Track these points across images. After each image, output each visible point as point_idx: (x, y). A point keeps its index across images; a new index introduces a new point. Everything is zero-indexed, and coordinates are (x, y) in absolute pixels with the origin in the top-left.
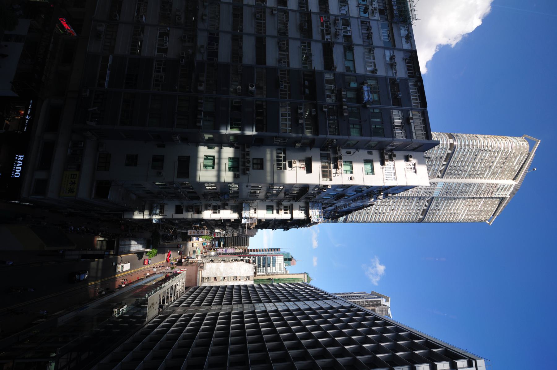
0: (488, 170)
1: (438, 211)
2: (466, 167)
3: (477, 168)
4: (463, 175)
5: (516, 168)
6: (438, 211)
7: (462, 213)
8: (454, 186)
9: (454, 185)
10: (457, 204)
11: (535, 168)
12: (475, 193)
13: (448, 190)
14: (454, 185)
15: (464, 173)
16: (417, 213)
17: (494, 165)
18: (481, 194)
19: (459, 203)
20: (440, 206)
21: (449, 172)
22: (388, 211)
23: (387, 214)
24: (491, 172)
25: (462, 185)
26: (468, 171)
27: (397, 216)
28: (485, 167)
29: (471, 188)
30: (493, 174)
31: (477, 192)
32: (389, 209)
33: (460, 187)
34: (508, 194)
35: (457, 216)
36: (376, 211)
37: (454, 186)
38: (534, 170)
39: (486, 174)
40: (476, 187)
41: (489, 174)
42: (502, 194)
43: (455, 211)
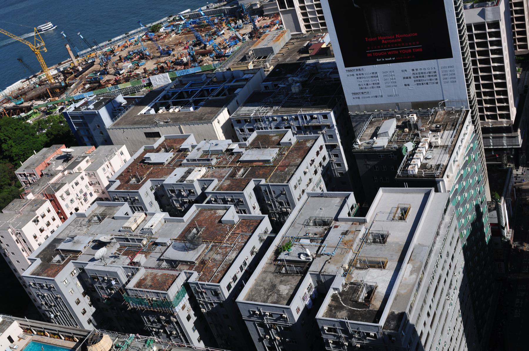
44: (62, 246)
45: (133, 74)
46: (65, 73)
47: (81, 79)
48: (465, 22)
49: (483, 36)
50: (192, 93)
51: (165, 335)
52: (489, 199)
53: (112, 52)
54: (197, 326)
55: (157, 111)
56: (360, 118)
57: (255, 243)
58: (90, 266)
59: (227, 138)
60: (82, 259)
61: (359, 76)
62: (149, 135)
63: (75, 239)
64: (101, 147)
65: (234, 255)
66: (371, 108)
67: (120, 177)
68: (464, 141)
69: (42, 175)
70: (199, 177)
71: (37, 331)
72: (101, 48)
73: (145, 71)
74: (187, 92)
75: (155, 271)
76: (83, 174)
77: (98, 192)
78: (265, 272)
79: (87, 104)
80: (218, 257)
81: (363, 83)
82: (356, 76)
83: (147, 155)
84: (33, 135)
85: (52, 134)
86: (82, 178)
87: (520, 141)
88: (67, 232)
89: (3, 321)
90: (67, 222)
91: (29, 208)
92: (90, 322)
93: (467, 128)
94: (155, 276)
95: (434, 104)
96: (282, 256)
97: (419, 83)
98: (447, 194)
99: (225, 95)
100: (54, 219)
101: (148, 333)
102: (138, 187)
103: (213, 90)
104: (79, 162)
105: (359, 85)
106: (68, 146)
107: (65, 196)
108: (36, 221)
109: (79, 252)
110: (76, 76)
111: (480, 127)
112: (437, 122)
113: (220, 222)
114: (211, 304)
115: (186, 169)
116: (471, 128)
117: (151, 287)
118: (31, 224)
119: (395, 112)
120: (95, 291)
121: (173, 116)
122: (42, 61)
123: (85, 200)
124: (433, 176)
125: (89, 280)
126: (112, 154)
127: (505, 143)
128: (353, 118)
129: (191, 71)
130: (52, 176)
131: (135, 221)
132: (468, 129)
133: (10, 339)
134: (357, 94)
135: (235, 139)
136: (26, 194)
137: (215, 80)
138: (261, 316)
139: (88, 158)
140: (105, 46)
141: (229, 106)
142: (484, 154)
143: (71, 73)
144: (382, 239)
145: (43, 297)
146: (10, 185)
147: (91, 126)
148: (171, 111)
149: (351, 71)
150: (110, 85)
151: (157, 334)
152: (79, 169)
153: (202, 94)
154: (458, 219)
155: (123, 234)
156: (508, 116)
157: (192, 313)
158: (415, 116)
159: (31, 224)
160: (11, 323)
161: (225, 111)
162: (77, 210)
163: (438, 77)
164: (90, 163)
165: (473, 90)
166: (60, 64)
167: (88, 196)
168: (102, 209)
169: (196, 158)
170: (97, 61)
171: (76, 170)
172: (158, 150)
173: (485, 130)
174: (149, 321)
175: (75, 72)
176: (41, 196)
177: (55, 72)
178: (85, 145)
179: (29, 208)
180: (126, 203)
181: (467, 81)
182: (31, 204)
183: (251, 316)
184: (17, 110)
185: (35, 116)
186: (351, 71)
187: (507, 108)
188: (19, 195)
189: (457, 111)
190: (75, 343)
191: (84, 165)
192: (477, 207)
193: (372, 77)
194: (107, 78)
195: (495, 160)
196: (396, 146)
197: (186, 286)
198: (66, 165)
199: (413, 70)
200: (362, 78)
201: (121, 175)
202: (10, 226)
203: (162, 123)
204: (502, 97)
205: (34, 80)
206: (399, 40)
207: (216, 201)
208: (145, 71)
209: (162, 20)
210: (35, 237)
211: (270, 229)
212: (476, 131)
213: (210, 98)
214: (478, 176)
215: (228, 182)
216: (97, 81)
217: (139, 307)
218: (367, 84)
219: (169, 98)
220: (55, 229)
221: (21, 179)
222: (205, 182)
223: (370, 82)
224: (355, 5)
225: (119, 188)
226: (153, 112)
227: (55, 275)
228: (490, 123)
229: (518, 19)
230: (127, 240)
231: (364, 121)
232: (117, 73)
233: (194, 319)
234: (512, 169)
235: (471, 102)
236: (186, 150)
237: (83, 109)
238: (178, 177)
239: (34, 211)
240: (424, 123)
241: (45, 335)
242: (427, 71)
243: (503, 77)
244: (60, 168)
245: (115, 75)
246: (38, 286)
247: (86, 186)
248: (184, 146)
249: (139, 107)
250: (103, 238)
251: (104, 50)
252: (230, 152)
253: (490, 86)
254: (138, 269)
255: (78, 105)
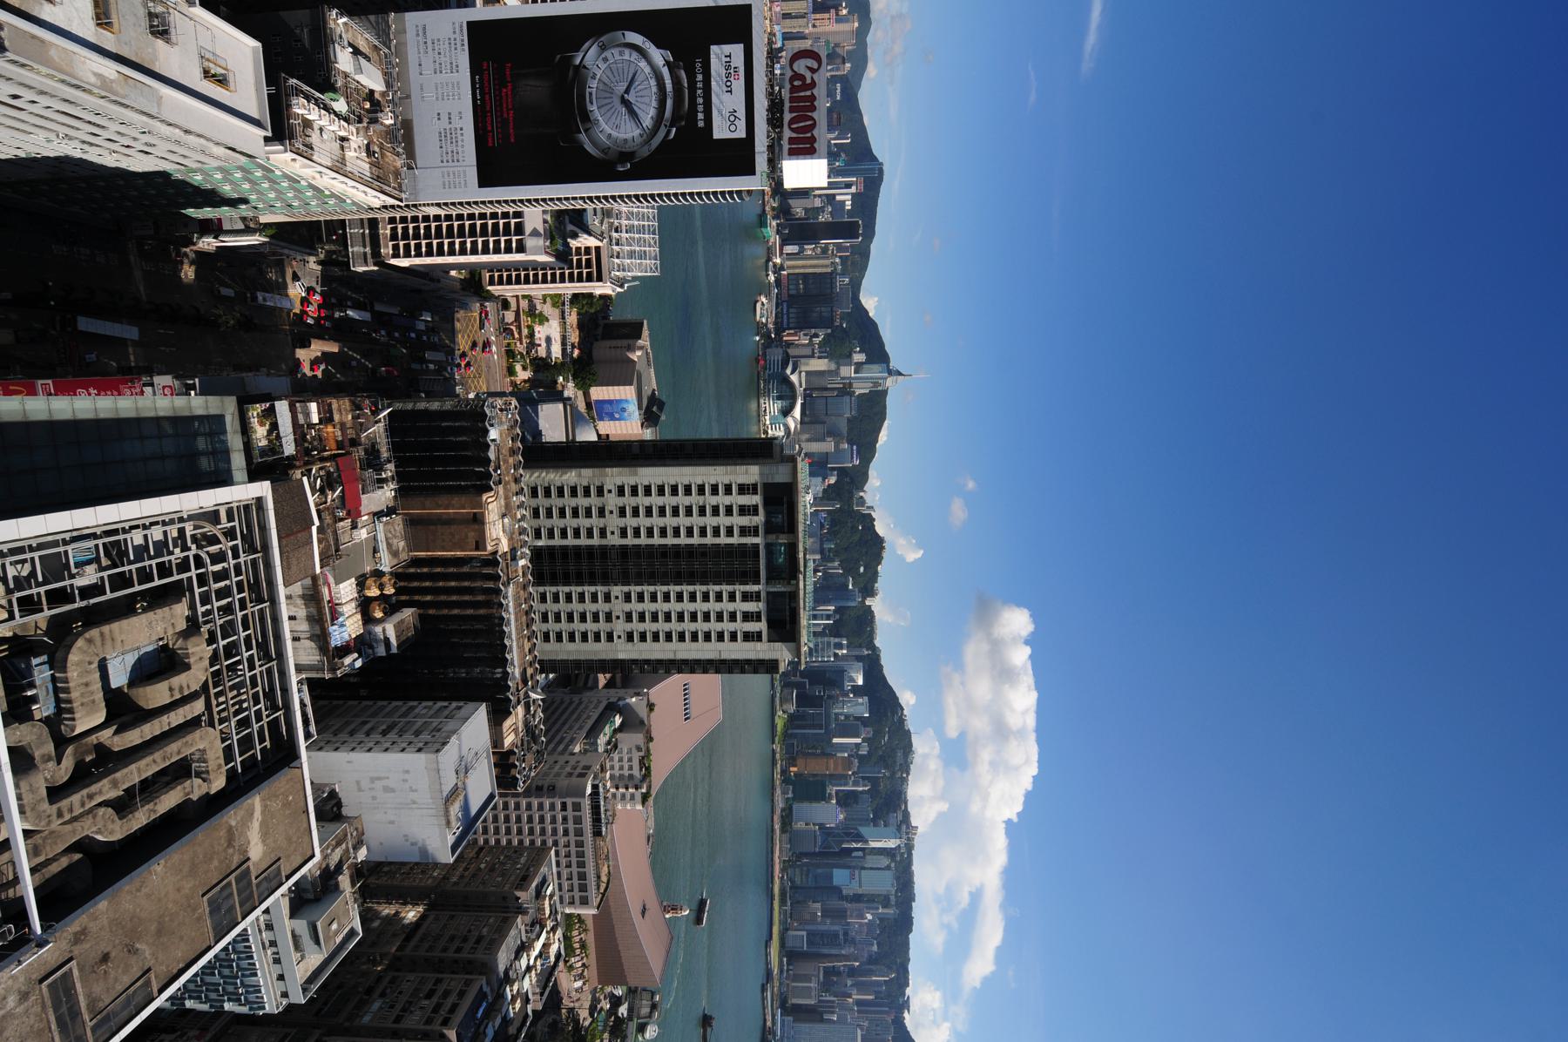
48: (524, 209)
49: (507, 231)
52: (264, 219)
56: (384, 31)
61: (453, 42)
66: (400, 51)
68: (354, 191)
81: (442, 47)
82: (452, 37)
87: (361, 269)
93: (375, 197)
95: (410, 153)
97: (444, 136)
98: (264, 156)
105: (439, 40)
111: (377, 216)
112: (383, 155)
116: (376, 203)
119: (396, 92)
124: (291, 137)
127: (355, 249)
128: (383, 18)
132: (374, 199)
134: (425, 33)
142: (335, 218)
144: (160, 30)
149: (461, 30)
154: (220, 169)
156: (396, 255)
158: (392, 122)
163: (451, 164)
165: (433, 211)
173: (373, 223)
181: (446, 204)
186: (461, 30)
187: (407, 255)
189: (400, 185)
192: (245, 201)
193: (451, 63)
195: (329, 235)
196: (339, 84)
199: (461, 129)
200: (450, 51)
204: (424, 249)
206: (505, 115)
212: (372, 209)
214: (300, 207)
218: (439, 53)
223: (443, 59)
224: (559, 56)
228: (385, 231)
229: (527, 276)
231: (378, 36)
234: (317, 255)
235: (415, 206)
240: (380, 135)
242: (460, 149)
243: (452, 253)
253: (439, 234)
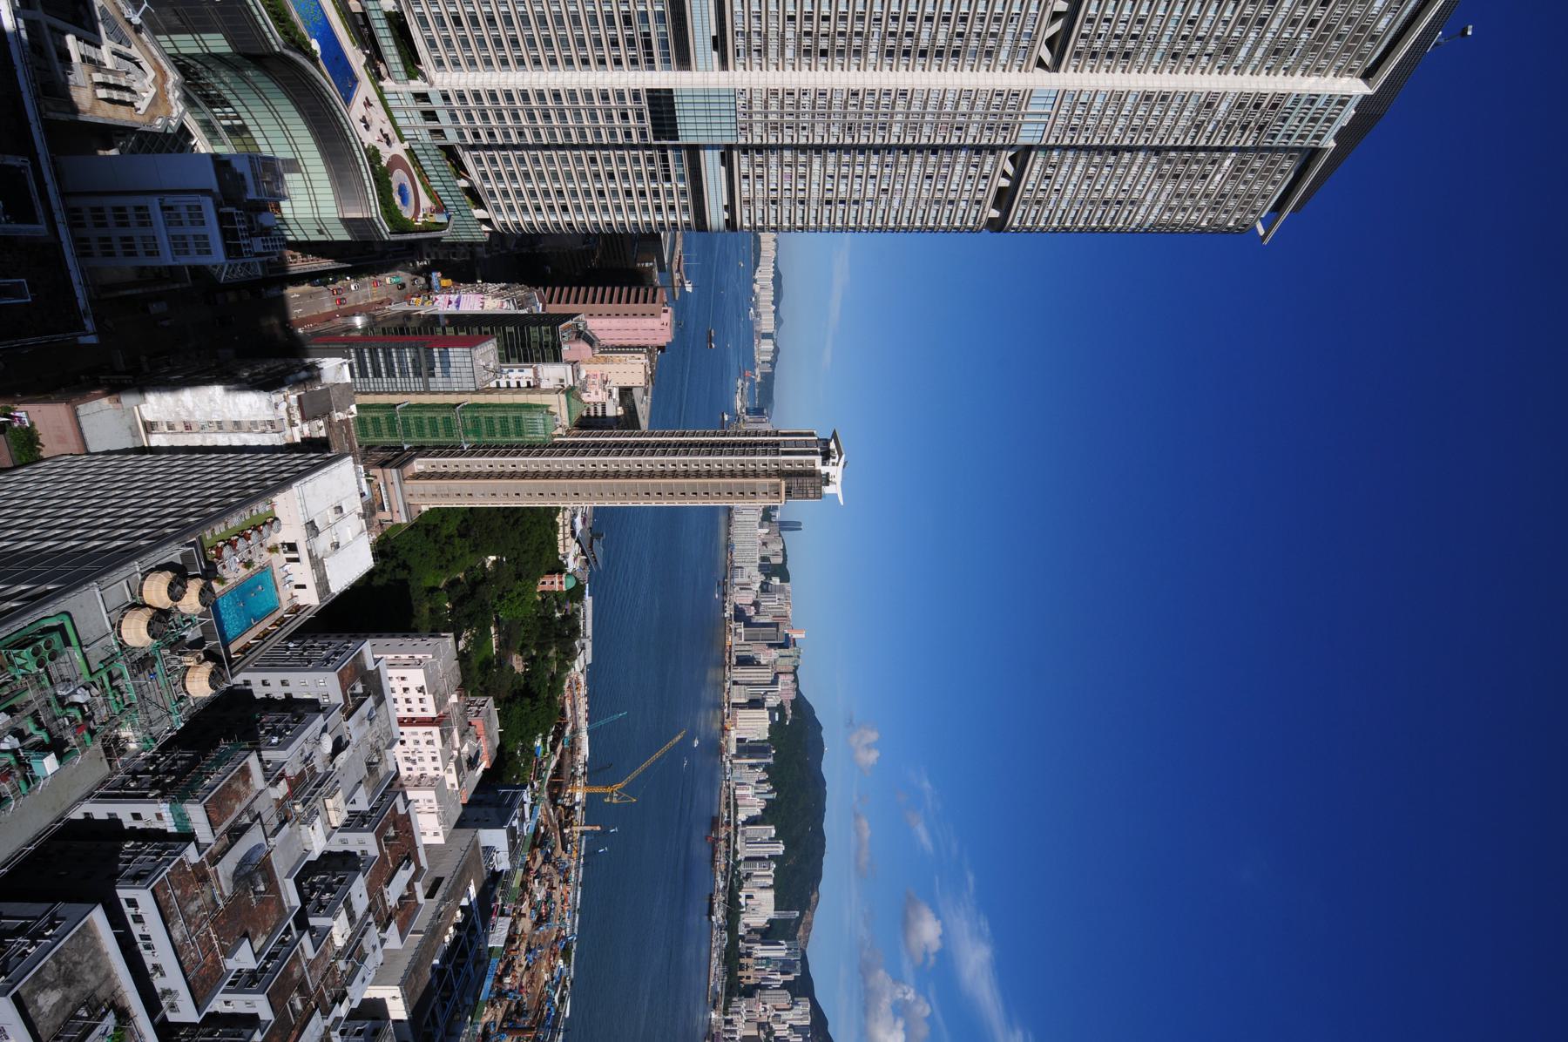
0: (1252, 35)
1: (1054, 196)
2: (1156, 23)
3: (1206, 24)
4: (1143, 55)
5: (1383, 24)
6: (1054, 196)
7: (1147, 203)
8: (1098, 104)
9: (1099, 100)
10: (1128, 167)
11: (1470, 27)
12: (1189, 128)
13: (1075, 121)
14: (1099, 100)
15: (1146, 47)
16: (978, 202)
17: (1281, 14)
18: (1212, 133)
19: (1135, 169)
20: (1060, 179)
21: (1082, 43)
22: (870, 195)
23: (868, 205)
24: (1265, 45)
25: (1130, 99)
26: (1165, 39)
27: (1059, 213)
28: (1243, 21)
29: (1171, 113)
30: (1277, 52)
31: (1198, 127)
32: (870, 187)
33: (1123, 105)
34: (1330, 131)
35: (1130, 212)
36: (828, 195)
37: (1098, 104)
38: (1465, 30)
39: (1243, 53)
40: (1190, 106)
41: (1259, 54)
42: (1301, 137)
43: (1122, 196)
44: (370, 702)
45: (527, 896)
46: (570, 810)
47: (554, 826)
50: (457, 973)
51: (140, 769)
53: (566, 881)
54: (114, 822)
55: (463, 909)
57: (171, 979)
58: (320, 721)
59: (364, 1001)
60: (337, 716)
62: (437, 882)
63: (368, 723)
64: (460, 810)
65: (177, 935)
67: (407, 818)
69: (470, 724)
70: (334, 931)
71: (286, 619)
72: (577, 868)
73: (522, 915)
74: (462, 965)
75: (246, 802)
76: (441, 773)
77: (407, 779)
78: (109, 976)
79: (522, 819)
80: (193, 907)
83: (413, 868)
84: (522, 738)
85: (510, 759)
86: (436, 769)
88: (383, 717)
89: (329, 591)
90: (395, 723)
91: (441, 690)
92: (247, 683)
94: (240, 800)
96: (110, 1021)
99: (428, 1024)
100: (409, 710)
101: (163, 749)
102: (378, 836)
103: (444, 1007)
104: (458, 775)
106: (485, 771)
107: (429, 737)
108: (421, 690)
109: (348, 718)
110: (560, 821)
113: (246, 935)
114: (129, 861)
115: (359, 916)
117: (229, 785)
118: (422, 682)
120: (282, 711)
121: (442, 927)
122: (597, 790)
123: (407, 759)
125: (302, 711)
126: (443, 820)
129: (488, 983)
130: (462, 736)
131: (336, 809)
133: (303, 587)
135: (353, 1015)
136: (459, 696)
137: (457, 1017)
138: (35, 937)
139: (457, 788)
140: (577, 875)
141: (407, 1024)
143: (566, 817)
145: (323, 648)
146: (481, 684)
147: (492, 811)
148: (451, 930)
150: (528, 858)
151: (153, 760)
152: (450, 771)
153: (448, 988)
155: (331, 784)
157: (139, 825)
159: (422, 682)
160: (320, 599)
161: (403, 1015)
162: (403, 742)
164: (449, 787)
166: (584, 809)
167: (409, 765)
168: (382, 772)
169: (365, 939)
170: (565, 857)
171: (452, 766)
172: (410, 886)
174: (181, 759)
175: (566, 821)
176: (447, 710)
177: (577, 799)
178: (474, 793)
179: (441, 690)
180: (368, 809)
182: (445, 694)
183: (54, 917)
184: (559, 735)
185: (541, 750)
188: (464, 687)
190: (232, 651)
191: (451, 778)
194: (540, 859)
197: (188, 837)
198: (464, 757)
201: (409, 820)
202: (435, 660)
203: (442, 909)
205: (581, 770)
207: (282, 942)
208: (522, 915)
209: (572, 969)
210: (403, 679)
211: (172, 1017)
213: (435, 998)
215: (296, 973)
216: (542, 844)
217: (214, 755)
219: (468, 934)
220: (396, 706)
221: (480, 700)
222: (322, 936)
225: (395, 808)
226: (465, 902)
227: (341, 676)
230: (319, 785)
232: (538, 875)
233: (128, 822)
236: (385, 928)
237: (518, 811)
238: (355, 899)
239: (434, 694)
241: (274, 624)
244: (466, 749)
245: (537, 871)
246: (341, 650)
247: (423, 769)
248: (393, 927)
249: (481, 885)
250: (343, 756)
251: (573, 871)
252: (340, 998)
254: (267, 779)
255: (527, 807)
